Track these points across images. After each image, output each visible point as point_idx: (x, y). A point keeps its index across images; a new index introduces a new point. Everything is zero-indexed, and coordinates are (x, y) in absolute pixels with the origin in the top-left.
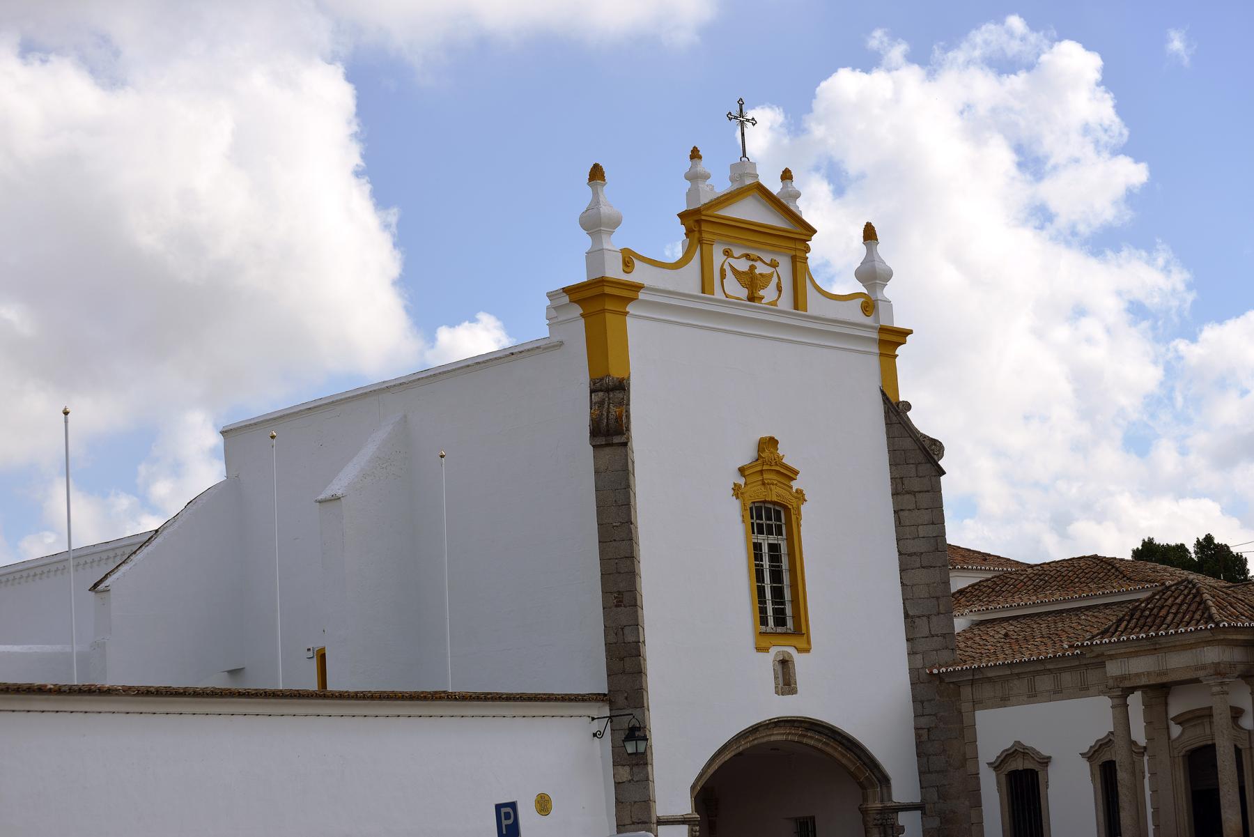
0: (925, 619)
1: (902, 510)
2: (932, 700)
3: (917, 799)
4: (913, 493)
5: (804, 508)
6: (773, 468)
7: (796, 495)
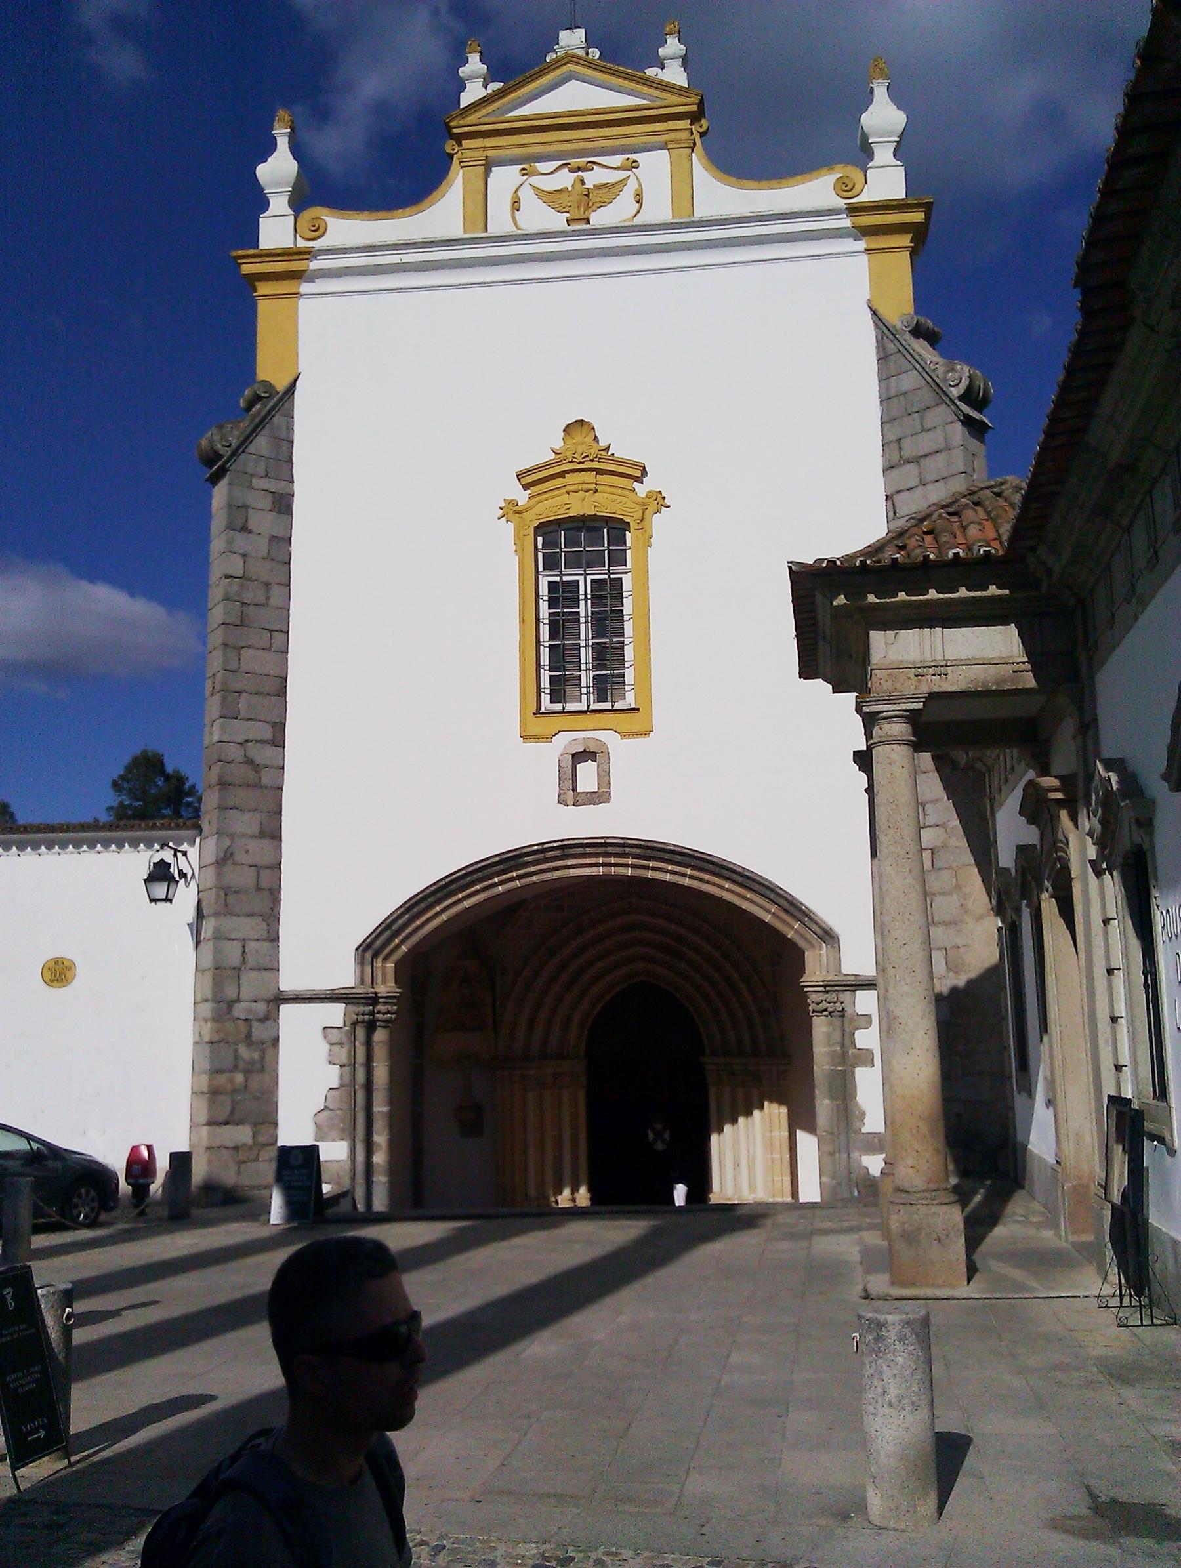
1: (899, 492)
4: (916, 460)
5: (659, 523)
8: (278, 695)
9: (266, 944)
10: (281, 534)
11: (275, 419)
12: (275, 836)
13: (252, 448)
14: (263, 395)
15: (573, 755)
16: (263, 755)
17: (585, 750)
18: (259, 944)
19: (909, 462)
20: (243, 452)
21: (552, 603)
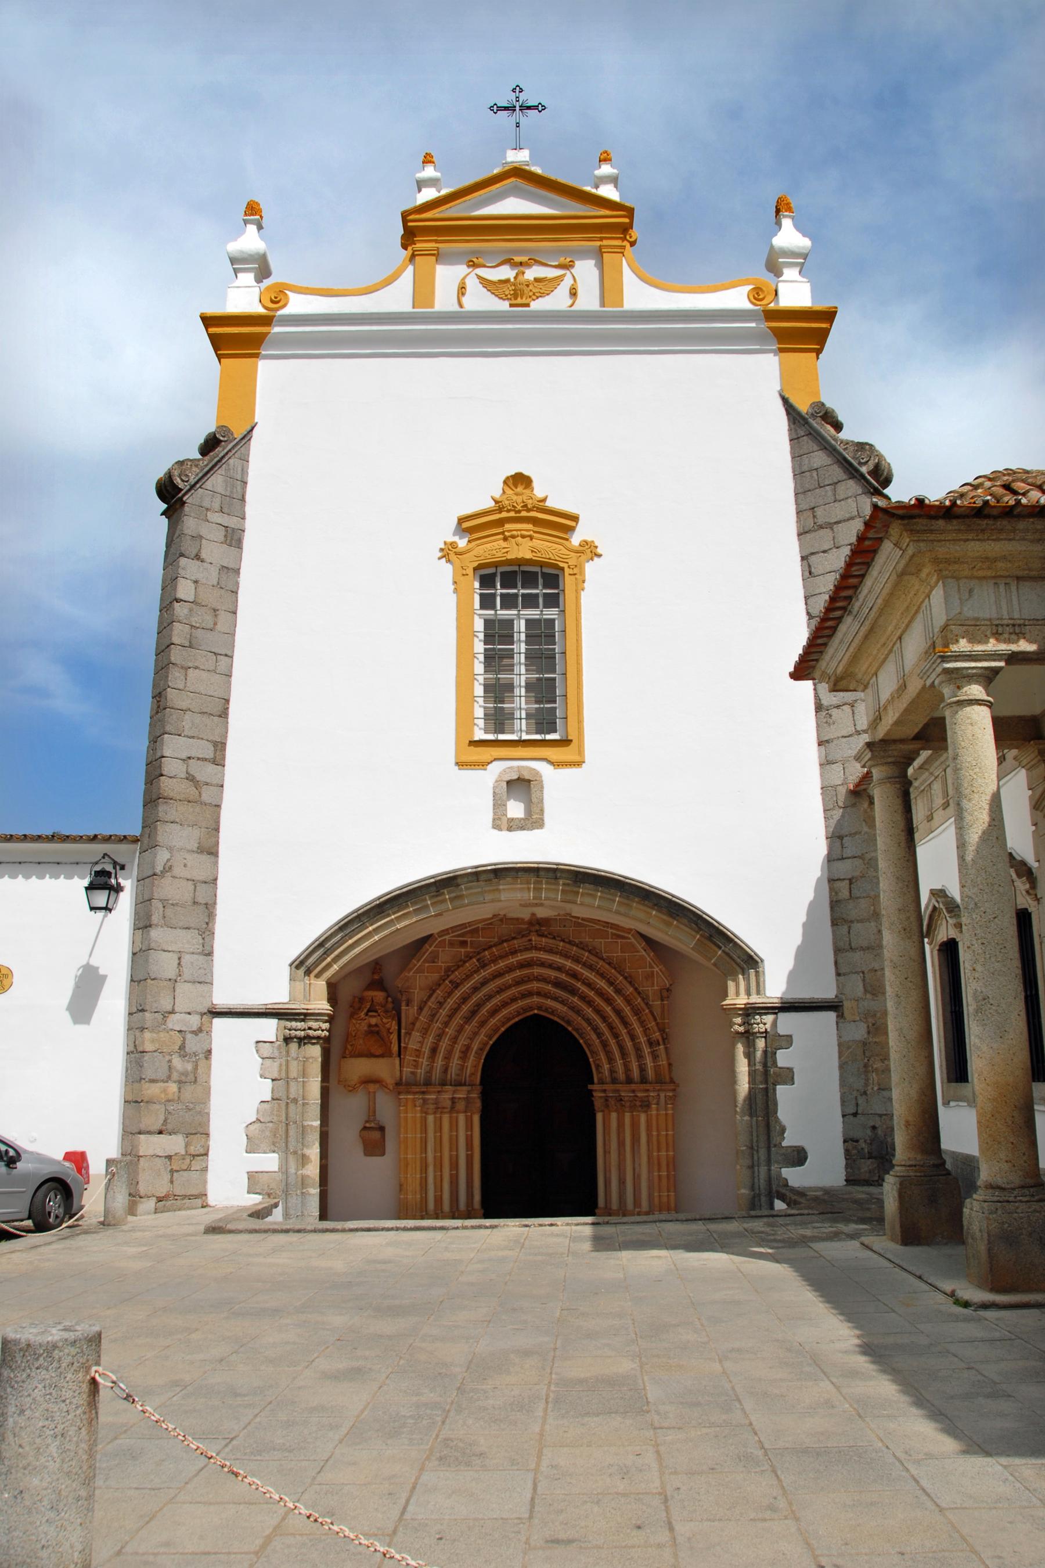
0: (847, 708)
1: (813, 554)
2: (856, 833)
3: (828, 991)
4: (830, 526)
5: (591, 568)
6: (524, 514)
7: (582, 548)
8: (220, 716)
9: (202, 957)
10: (231, 566)
11: (231, 461)
12: (211, 851)
13: (209, 485)
14: (222, 438)
15: (508, 782)
16: (205, 772)
17: (519, 779)
18: (196, 956)
19: (821, 527)
20: (200, 487)
21: (488, 639)
